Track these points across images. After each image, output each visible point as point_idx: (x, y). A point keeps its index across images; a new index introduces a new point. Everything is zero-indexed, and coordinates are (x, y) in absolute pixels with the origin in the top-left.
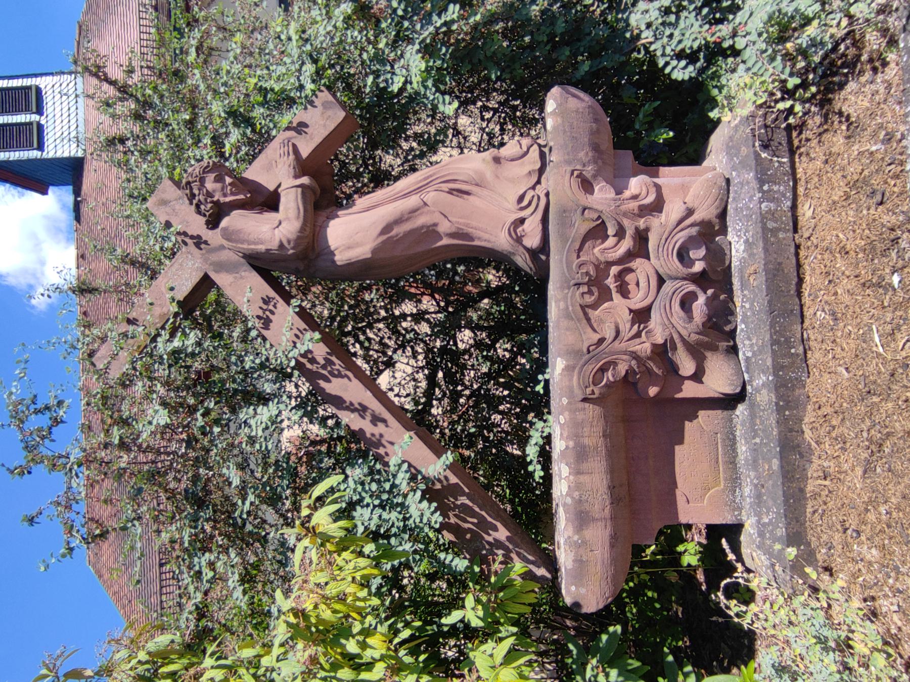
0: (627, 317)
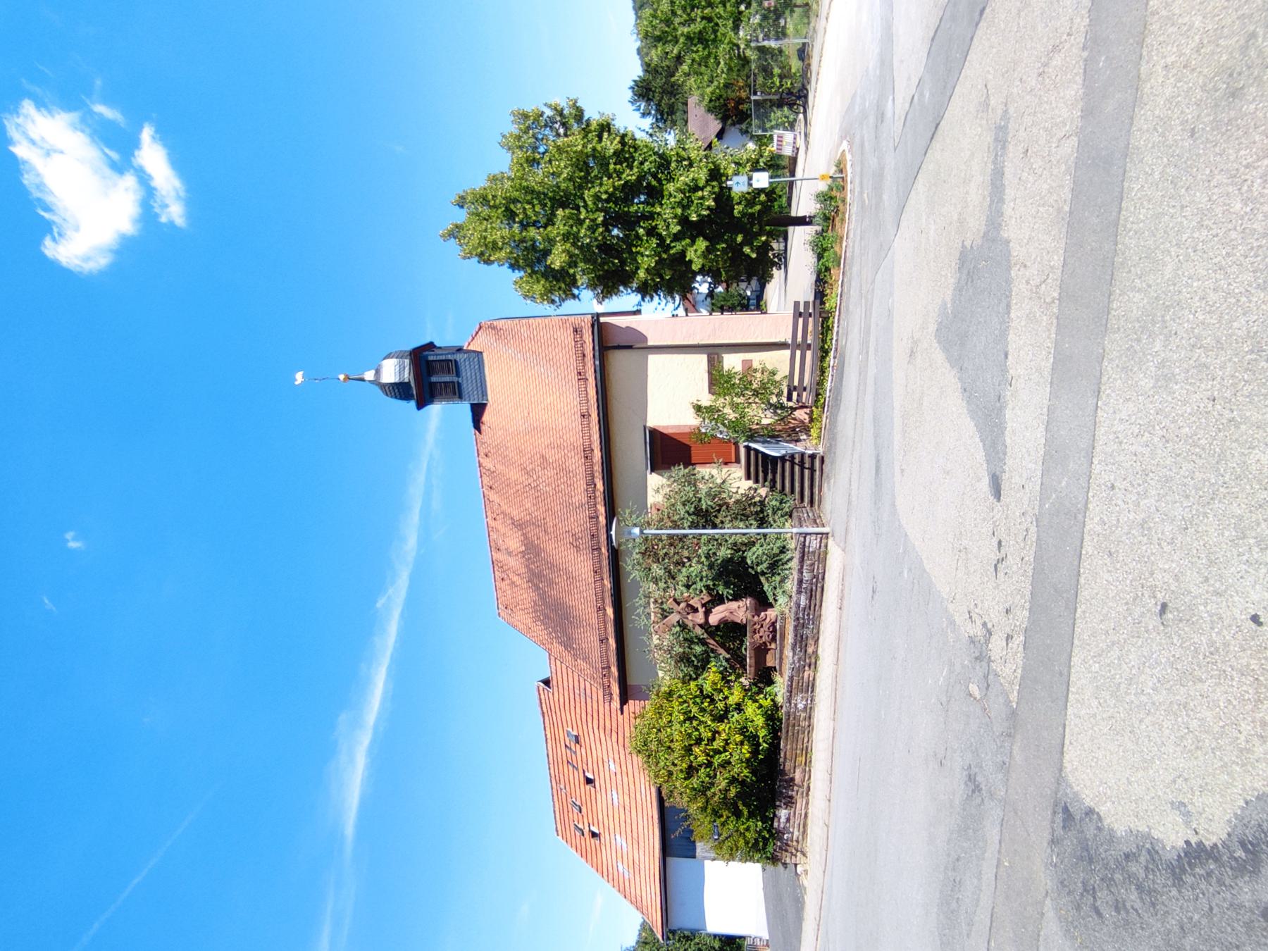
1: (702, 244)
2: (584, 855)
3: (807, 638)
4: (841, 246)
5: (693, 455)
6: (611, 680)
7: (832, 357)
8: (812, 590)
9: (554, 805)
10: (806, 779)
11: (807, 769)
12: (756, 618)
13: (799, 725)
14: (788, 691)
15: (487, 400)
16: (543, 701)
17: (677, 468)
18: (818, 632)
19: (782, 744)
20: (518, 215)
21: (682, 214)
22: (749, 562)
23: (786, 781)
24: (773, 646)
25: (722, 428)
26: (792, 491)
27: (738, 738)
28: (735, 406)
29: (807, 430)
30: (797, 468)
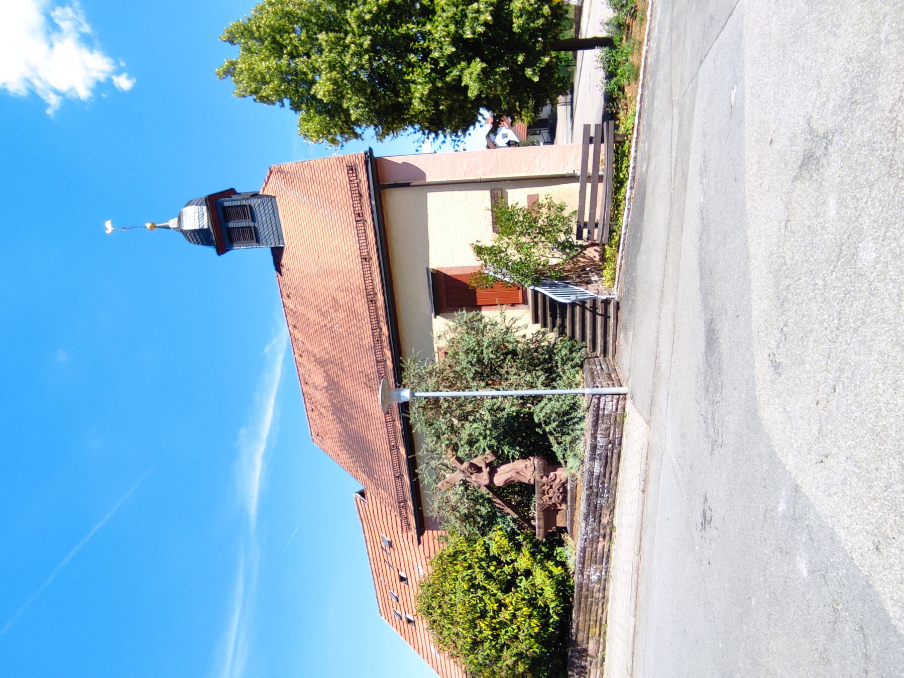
0: (548, 498)
1: (478, 65)
2: (403, 633)
3: (601, 507)
4: (640, 54)
5: (478, 297)
6: (408, 511)
7: (628, 188)
8: (607, 456)
9: (376, 592)
10: (601, 650)
11: (602, 640)
12: (545, 479)
13: (592, 597)
14: (580, 557)
15: (284, 244)
16: (361, 510)
17: (459, 313)
18: (614, 502)
19: (574, 616)
20: (286, 47)
21: (456, 31)
22: (536, 420)
23: (579, 652)
24: (563, 506)
25: (504, 271)
26: (583, 338)
27: (526, 610)
28: (519, 247)
29: (599, 270)
30: (588, 314)
